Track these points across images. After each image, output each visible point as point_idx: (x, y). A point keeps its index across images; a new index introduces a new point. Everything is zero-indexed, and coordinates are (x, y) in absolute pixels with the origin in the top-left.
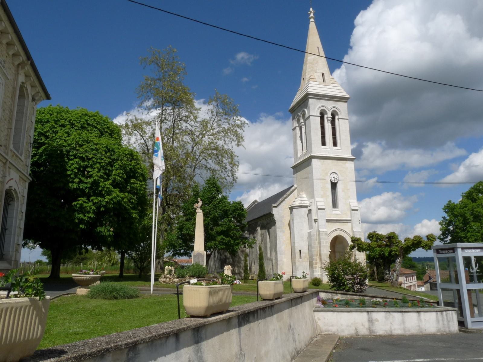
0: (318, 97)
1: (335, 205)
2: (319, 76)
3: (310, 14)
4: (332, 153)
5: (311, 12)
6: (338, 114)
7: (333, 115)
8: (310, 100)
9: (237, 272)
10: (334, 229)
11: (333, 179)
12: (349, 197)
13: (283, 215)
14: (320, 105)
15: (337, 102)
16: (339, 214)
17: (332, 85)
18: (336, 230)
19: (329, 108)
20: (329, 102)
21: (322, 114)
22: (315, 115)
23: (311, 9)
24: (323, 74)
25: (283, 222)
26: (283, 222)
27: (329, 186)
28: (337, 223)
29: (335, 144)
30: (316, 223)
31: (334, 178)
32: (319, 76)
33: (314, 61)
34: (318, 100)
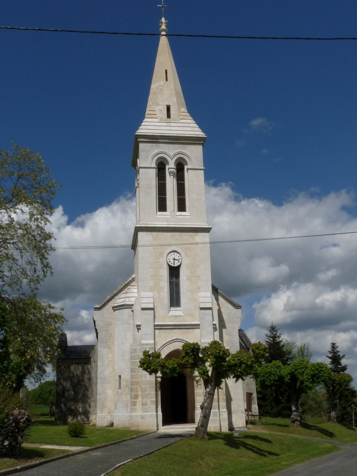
0: (154, 139)
1: (175, 300)
2: (161, 111)
3: (161, 26)
4: (174, 222)
5: (162, 23)
6: (187, 164)
7: (180, 166)
8: (141, 145)
9: (81, 410)
10: (170, 340)
11: (172, 261)
12: (199, 288)
13: (110, 321)
14: (157, 151)
15: (186, 146)
16: (181, 316)
17: (181, 121)
18: (173, 341)
19: (171, 155)
20: (171, 146)
21: (161, 166)
22: (148, 166)
23: (163, 20)
24: (168, 108)
25: (110, 332)
26: (110, 332)
27: (165, 273)
28: (175, 330)
29: (182, 207)
30: (139, 331)
31: (174, 259)
32: (161, 111)
33: (157, 89)
34: (154, 145)
